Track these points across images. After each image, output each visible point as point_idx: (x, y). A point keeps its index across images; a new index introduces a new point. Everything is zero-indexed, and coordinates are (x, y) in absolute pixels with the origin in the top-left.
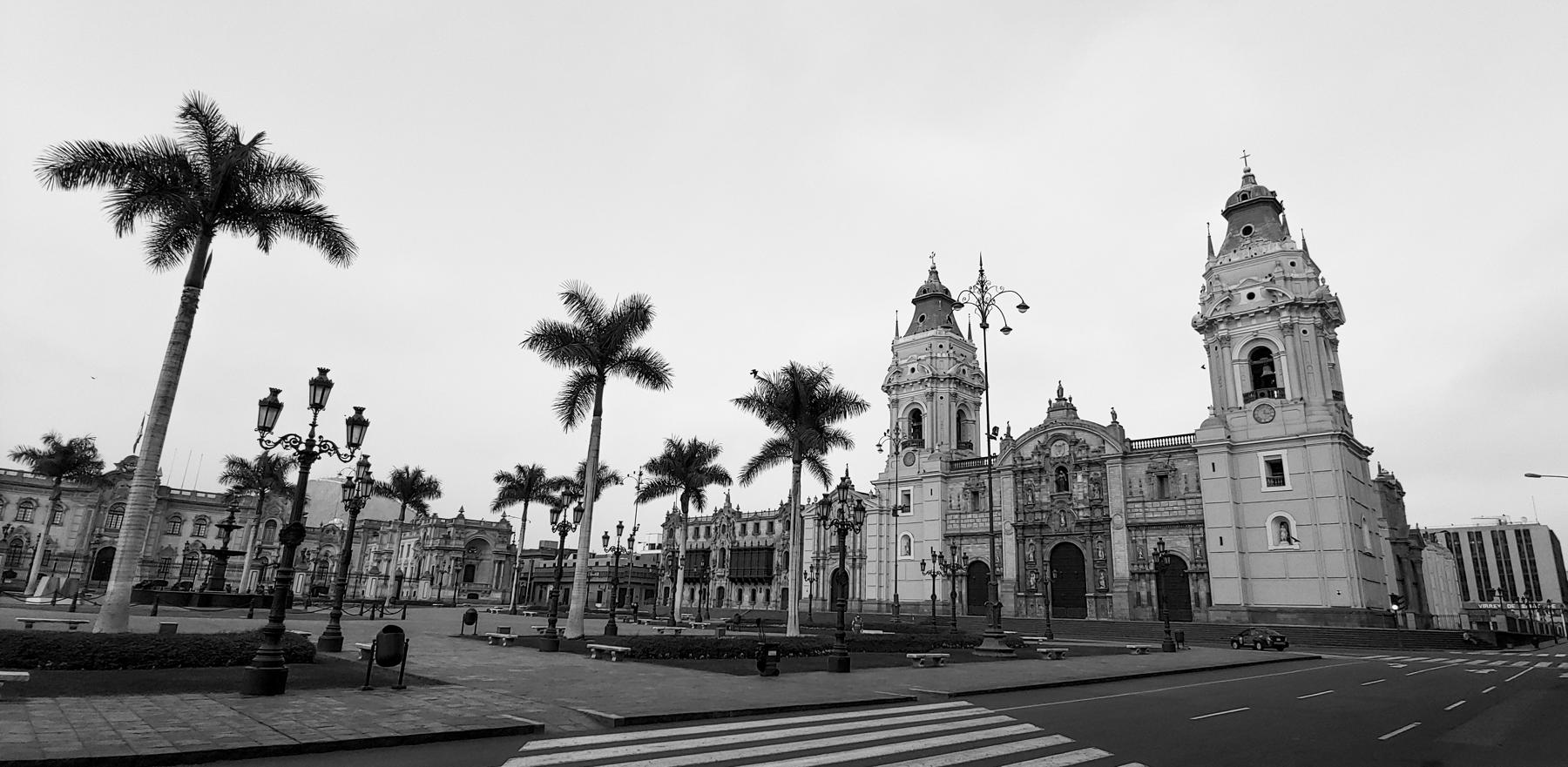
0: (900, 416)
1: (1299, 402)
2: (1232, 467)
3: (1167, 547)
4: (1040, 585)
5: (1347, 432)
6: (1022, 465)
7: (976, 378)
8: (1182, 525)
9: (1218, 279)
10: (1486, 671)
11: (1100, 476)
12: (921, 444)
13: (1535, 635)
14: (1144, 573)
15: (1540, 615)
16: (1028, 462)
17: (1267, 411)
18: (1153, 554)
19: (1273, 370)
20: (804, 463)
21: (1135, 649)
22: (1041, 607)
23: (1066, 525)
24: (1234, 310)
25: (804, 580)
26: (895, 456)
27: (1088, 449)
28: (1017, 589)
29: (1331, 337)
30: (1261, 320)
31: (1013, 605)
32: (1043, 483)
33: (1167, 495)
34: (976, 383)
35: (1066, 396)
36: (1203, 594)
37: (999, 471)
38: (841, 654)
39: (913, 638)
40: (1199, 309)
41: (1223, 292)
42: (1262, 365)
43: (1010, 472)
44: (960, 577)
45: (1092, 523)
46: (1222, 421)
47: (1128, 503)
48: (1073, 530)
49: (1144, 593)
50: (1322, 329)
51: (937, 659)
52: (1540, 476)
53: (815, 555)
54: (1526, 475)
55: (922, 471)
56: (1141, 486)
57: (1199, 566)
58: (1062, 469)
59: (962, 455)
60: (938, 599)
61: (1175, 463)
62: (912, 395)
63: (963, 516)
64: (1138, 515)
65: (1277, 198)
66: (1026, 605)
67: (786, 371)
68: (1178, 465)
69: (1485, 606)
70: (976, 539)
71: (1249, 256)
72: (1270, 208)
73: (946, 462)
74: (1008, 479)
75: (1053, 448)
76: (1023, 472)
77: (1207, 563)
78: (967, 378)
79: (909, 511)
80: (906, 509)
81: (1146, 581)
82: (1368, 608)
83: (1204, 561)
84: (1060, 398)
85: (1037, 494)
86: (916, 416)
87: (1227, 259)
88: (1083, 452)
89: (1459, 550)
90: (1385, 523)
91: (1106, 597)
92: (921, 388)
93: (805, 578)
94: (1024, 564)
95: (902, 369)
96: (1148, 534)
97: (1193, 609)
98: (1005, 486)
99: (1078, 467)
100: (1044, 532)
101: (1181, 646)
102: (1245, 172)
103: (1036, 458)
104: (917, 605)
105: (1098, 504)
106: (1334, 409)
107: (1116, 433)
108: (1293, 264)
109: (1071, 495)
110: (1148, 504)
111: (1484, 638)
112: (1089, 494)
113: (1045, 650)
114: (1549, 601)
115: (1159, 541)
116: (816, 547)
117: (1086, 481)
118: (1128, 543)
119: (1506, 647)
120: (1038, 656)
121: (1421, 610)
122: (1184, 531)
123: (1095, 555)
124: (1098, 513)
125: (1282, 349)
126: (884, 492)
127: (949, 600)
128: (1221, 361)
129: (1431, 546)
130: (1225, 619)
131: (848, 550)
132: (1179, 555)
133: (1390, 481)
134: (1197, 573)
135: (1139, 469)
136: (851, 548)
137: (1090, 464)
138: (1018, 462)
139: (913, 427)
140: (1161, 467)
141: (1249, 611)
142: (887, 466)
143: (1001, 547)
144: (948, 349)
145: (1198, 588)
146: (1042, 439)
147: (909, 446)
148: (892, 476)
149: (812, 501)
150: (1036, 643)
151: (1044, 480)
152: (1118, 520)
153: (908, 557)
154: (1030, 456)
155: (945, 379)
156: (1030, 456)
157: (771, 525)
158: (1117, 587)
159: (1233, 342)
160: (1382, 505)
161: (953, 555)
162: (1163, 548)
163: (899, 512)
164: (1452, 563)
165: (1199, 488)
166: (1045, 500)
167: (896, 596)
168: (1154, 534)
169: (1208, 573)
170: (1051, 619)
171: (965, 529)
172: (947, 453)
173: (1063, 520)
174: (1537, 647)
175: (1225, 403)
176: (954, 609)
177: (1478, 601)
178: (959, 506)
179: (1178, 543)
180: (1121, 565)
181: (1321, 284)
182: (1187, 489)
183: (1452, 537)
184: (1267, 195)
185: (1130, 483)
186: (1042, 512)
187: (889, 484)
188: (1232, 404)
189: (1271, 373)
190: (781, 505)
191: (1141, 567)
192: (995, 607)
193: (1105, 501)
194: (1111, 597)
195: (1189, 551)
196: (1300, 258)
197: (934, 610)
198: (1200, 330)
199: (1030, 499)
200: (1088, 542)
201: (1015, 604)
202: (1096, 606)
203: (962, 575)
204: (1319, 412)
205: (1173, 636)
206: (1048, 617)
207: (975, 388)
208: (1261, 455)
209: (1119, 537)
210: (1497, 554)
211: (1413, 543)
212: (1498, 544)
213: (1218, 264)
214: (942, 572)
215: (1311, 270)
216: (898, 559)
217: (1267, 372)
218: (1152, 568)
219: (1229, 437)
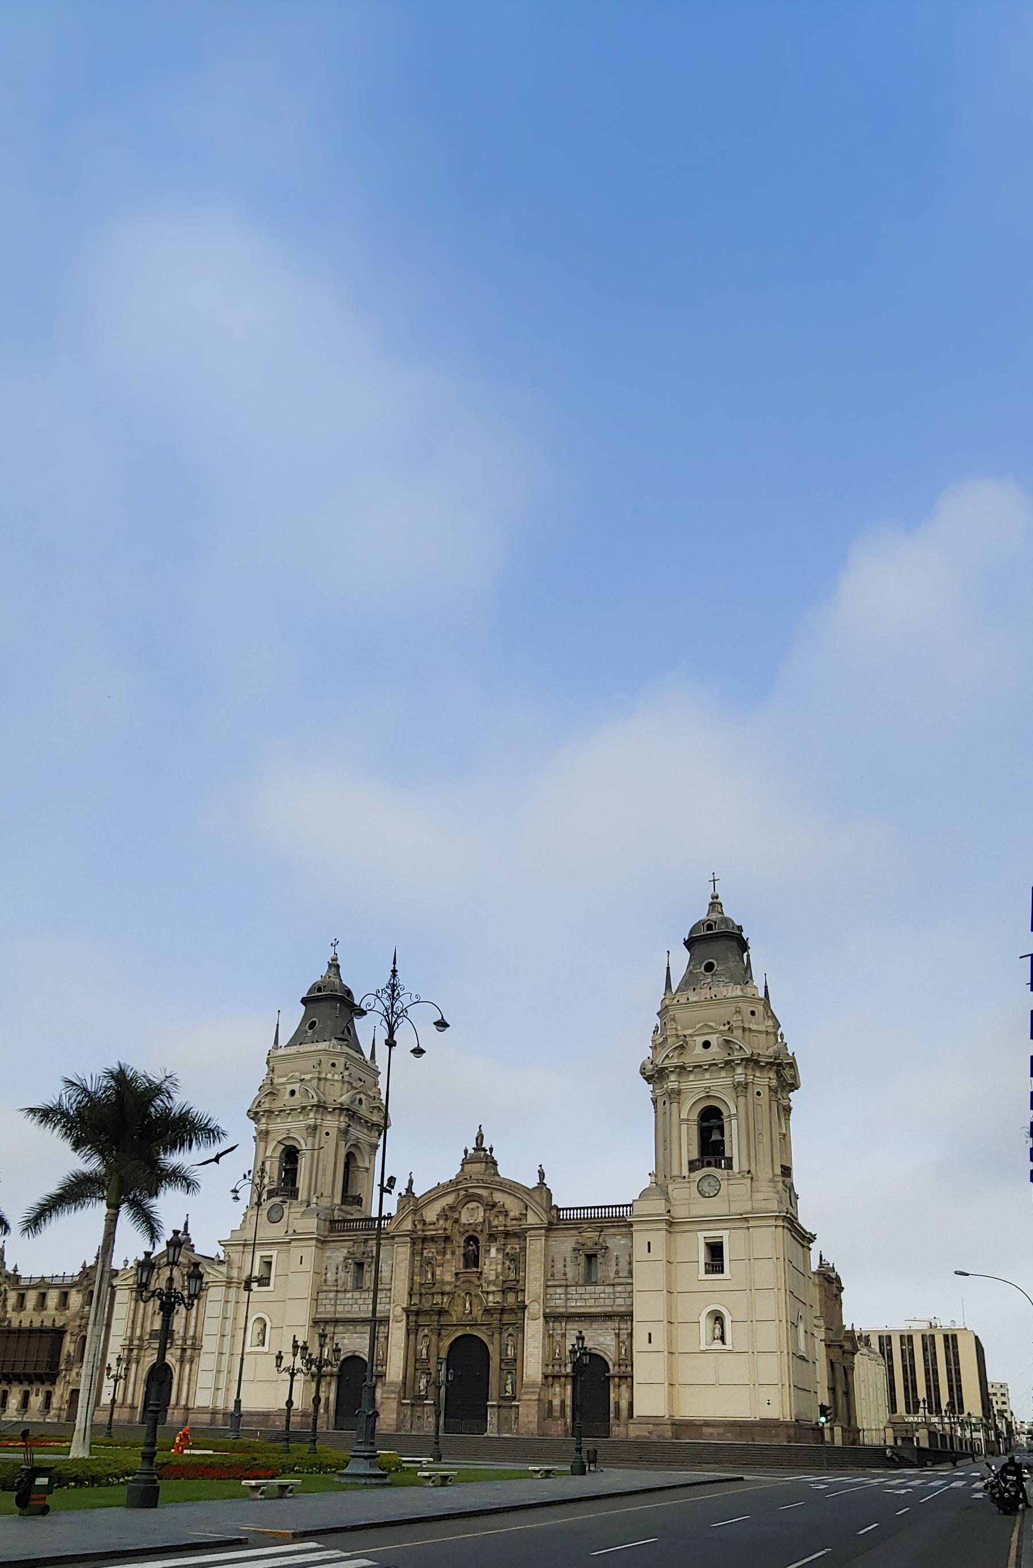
0: (268, 1154)
1: (746, 1176)
2: (669, 1247)
3: (588, 1344)
4: (431, 1389)
5: (791, 1214)
6: (423, 1231)
7: (376, 1111)
8: (608, 1317)
9: (673, 1020)
10: (903, 1492)
11: (518, 1250)
12: (294, 1194)
13: (955, 1453)
14: (559, 1377)
15: (961, 1430)
16: (432, 1227)
17: (713, 1183)
18: (570, 1352)
19: (722, 1134)
20: (124, 1209)
21: (538, 1472)
22: (430, 1419)
23: (471, 1311)
24: (688, 1060)
25: (106, 1377)
26: (256, 1207)
27: (506, 1215)
28: (402, 1395)
29: (785, 1102)
30: (716, 1075)
31: (395, 1416)
32: (448, 1256)
33: (593, 1280)
34: (374, 1119)
35: (486, 1145)
37: (393, 1238)
38: (146, 1481)
39: (255, 1459)
40: (650, 1054)
41: (677, 1036)
42: (712, 1128)
43: (408, 1239)
44: (328, 1378)
45: (503, 1311)
46: (663, 1191)
47: (548, 1286)
48: (479, 1320)
49: (556, 1402)
50: (777, 1093)
51: (283, 1488)
52: (967, 1275)
53: (127, 1342)
54: (956, 1273)
55: (291, 1231)
56: (565, 1266)
57: (623, 1368)
59: (347, 1213)
60: (295, 1406)
61: (607, 1239)
62: (287, 1126)
63: (340, 1295)
64: (558, 1304)
65: (743, 934)
66: (412, 1415)
67: (112, 1076)
68: (610, 1243)
69: (911, 1419)
71: (709, 998)
72: (735, 944)
73: (325, 1220)
74: (404, 1249)
75: (464, 1211)
76: (424, 1239)
77: (632, 1366)
78: (364, 1111)
79: (268, 1285)
80: (264, 1281)
81: (560, 1386)
82: (797, 1421)
83: (628, 1362)
84: (479, 1148)
85: (438, 1271)
86: (291, 1155)
87: (685, 997)
89: (890, 1357)
90: (821, 1323)
91: (511, 1407)
92: (301, 1118)
93: (108, 1375)
94: (415, 1363)
95: (278, 1090)
96: (568, 1327)
97: (611, 1421)
98: (400, 1257)
99: (493, 1238)
100: (444, 1320)
101: (593, 1468)
102: (712, 898)
103: (441, 1222)
104: (266, 1415)
105: (513, 1287)
106: (780, 1186)
107: (542, 1199)
108: (753, 1013)
109: (481, 1273)
111: (905, 1454)
112: (502, 1273)
113: (427, 1474)
114: (969, 1414)
115: (578, 1334)
116: (129, 1331)
117: (500, 1256)
118: (544, 1338)
119: (926, 1465)
120: (420, 1483)
121: (849, 1424)
123: (503, 1351)
124: (511, 1298)
126: (236, 1257)
127: (311, 1410)
128: (668, 1118)
129: (864, 1351)
130: (647, 1434)
131: (176, 1337)
132: (601, 1354)
133: (830, 1274)
134: (620, 1377)
135: (565, 1244)
136: (181, 1334)
137: (507, 1234)
138: (419, 1227)
139: (285, 1170)
140: (590, 1244)
141: (673, 1424)
142: (244, 1221)
143: (387, 1338)
144: (342, 1069)
145: (620, 1396)
146: (449, 1200)
147: (277, 1195)
148: (249, 1235)
149: (131, 1264)
150: (418, 1465)
151: (449, 1252)
152: (535, 1308)
153: (260, 1349)
154: (434, 1219)
156: (434, 1219)
157: (64, 1296)
158: (526, 1393)
159: (682, 1096)
160: (820, 1301)
161: (322, 1346)
162: (583, 1344)
163: (254, 1286)
164: (882, 1370)
165: (631, 1272)
166: (448, 1278)
167: (238, 1402)
169: (632, 1377)
170: (440, 1434)
171: (340, 1313)
172: (327, 1208)
173: (468, 1305)
174: (955, 1465)
175: (668, 1170)
176: (315, 1420)
177: (905, 1414)
178: (336, 1280)
179: (601, 1339)
180: (533, 1368)
181: (780, 1040)
182: (617, 1272)
183: (885, 1341)
184: (733, 928)
185: (553, 1261)
186: (443, 1294)
187: (244, 1245)
188: (675, 1172)
189: (720, 1138)
190: (84, 1267)
191: (557, 1368)
192: (369, 1416)
193: (521, 1282)
194: (517, 1407)
195: (613, 1349)
196: (761, 1008)
197: (288, 1421)
198: (648, 1079)
199: (430, 1276)
200: (497, 1336)
201: (398, 1414)
202: (498, 1418)
203: (331, 1375)
204: (765, 1189)
205: (584, 1455)
206: (437, 1433)
207: (373, 1125)
209: (534, 1329)
210: (926, 1361)
211: (847, 1346)
212: (927, 1350)
213: (675, 1002)
214: (304, 1368)
215: (770, 1023)
216: (247, 1349)
217: (715, 1137)
218: (569, 1369)
219: (669, 1211)
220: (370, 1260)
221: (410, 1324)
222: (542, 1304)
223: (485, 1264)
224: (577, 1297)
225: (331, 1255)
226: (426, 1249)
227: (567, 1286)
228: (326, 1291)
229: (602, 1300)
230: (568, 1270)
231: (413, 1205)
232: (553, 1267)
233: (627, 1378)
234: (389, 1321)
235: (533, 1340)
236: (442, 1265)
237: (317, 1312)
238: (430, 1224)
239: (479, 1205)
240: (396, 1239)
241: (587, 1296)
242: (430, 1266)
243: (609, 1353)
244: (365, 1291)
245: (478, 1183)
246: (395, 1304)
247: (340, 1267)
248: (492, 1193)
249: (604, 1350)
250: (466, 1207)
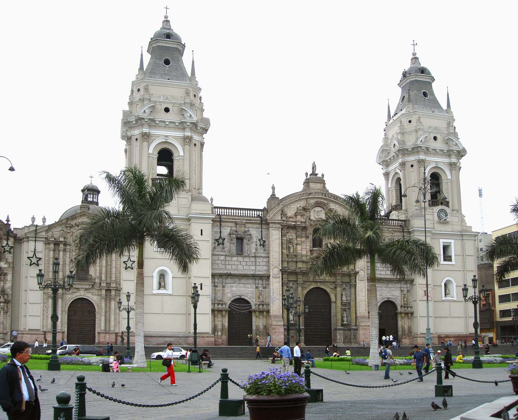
6: (288, 222)
36: (406, 327)
58: (316, 231)
63: (228, 258)
70: (240, 279)
74: (277, 232)
75: (312, 213)
76: (289, 227)
84: (314, 174)
85: (299, 247)
122: (398, 285)
125: (449, 177)
132: (394, 301)
146: (302, 204)
155: (201, 128)
166: (304, 253)
168: (380, 285)
179: (394, 293)
195: (399, 298)
200: (339, 289)
208: (442, 241)
220: (249, 237)
221: (284, 280)
224: (382, 269)
226: (288, 233)
228: (218, 255)
233: (410, 315)
234: (268, 277)
235: (362, 292)
237: (212, 269)
238: (290, 218)
239: (322, 210)
240: (271, 225)
242: (291, 244)
243: (398, 301)
244: (246, 257)
245: (323, 196)
246: (273, 267)
249: (394, 298)
250: (313, 209)
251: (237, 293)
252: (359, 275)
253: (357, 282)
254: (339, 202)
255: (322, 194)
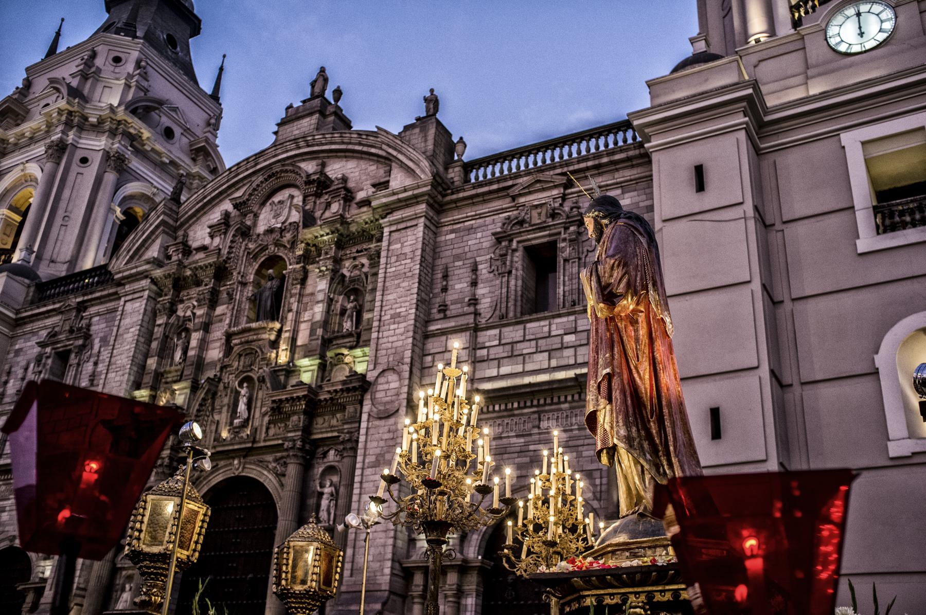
32: (220, 310)
56: (474, 284)
88: (335, 207)
98: (127, 321)
110: (489, 337)
112: (325, 324)
173: (242, 407)
222: (407, 375)
223: (290, 310)
225: (23, 345)
226: (182, 301)
227: (476, 329)
229: (570, 352)
230: (481, 290)
231: (164, 213)
232: (445, 289)
236: (206, 327)
241: (527, 348)
245: (299, 148)
247: (32, 366)
248: (323, 165)
251: (7, 529)
252: (379, 395)
253: (364, 425)
254: (350, 147)
255: (295, 140)
